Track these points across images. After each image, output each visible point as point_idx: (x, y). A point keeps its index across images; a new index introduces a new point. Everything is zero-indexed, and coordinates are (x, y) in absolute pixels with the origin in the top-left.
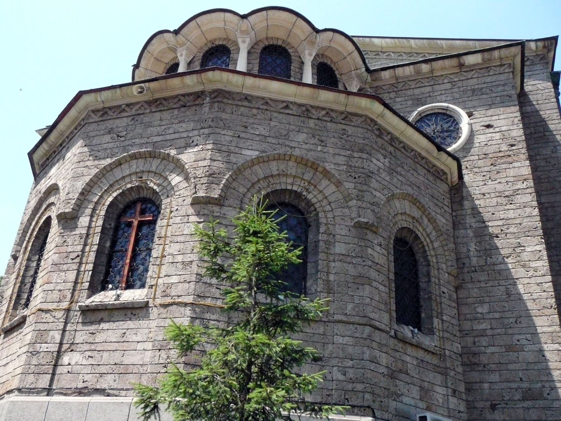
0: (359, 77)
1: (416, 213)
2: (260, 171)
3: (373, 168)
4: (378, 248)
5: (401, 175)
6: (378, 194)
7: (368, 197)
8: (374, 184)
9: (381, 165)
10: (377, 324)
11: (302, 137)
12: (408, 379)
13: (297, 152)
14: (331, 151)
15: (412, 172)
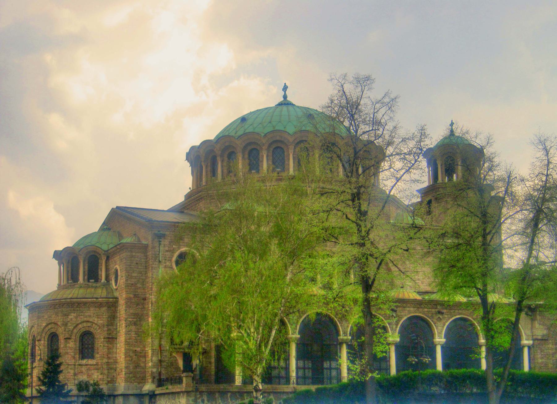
0: (104, 254)
1: (89, 324)
2: (47, 329)
3: (69, 319)
4: (71, 343)
5: (82, 315)
6: (70, 327)
7: (67, 330)
8: (69, 324)
9: (72, 317)
10: (70, 364)
11: (54, 316)
12: (82, 374)
13: (53, 321)
14: (60, 318)
15: (87, 311)
